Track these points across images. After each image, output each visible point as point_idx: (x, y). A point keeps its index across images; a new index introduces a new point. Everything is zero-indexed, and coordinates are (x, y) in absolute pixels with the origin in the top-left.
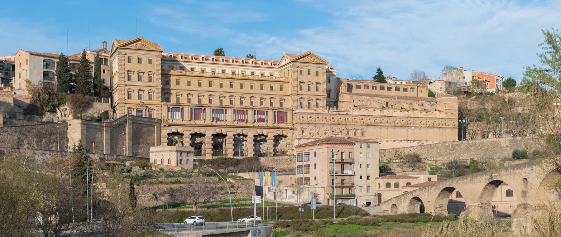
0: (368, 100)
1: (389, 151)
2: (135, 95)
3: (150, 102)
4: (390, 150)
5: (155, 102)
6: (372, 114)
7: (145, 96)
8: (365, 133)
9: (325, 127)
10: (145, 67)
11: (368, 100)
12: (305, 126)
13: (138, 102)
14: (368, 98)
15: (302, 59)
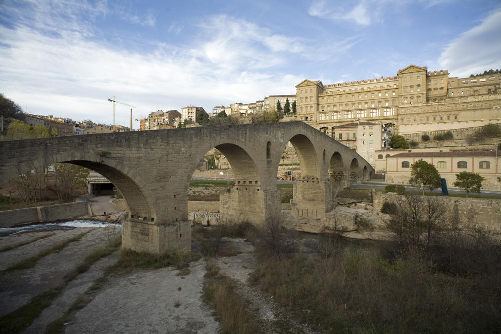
0: (469, 90)
1: (473, 130)
2: (304, 109)
3: (311, 112)
4: (474, 128)
5: (313, 112)
6: (465, 101)
7: (309, 109)
8: (458, 117)
9: (420, 115)
10: (309, 94)
11: (469, 90)
12: (404, 116)
13: (305, 113)
14: (468, 88)
15: (407, 70)
